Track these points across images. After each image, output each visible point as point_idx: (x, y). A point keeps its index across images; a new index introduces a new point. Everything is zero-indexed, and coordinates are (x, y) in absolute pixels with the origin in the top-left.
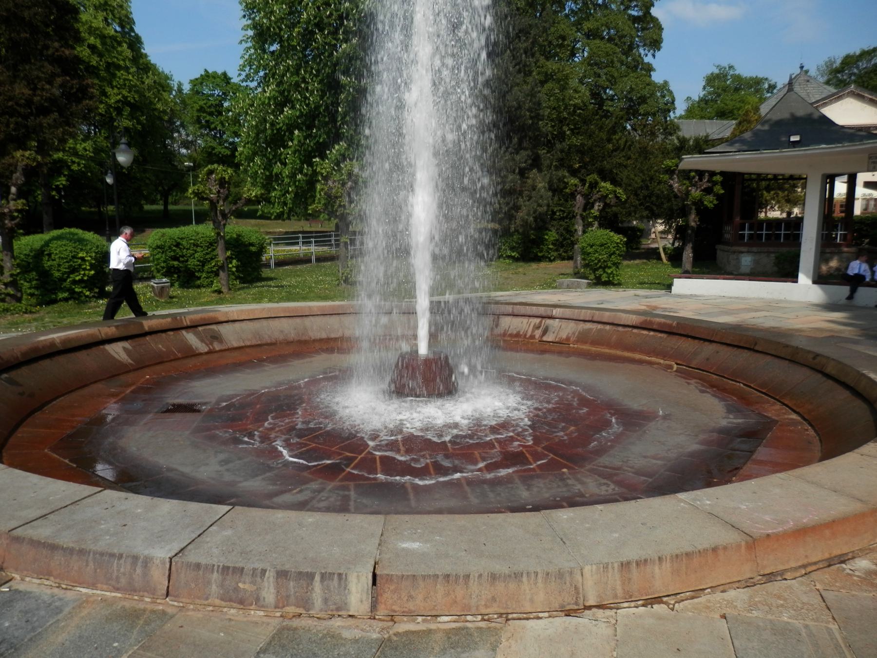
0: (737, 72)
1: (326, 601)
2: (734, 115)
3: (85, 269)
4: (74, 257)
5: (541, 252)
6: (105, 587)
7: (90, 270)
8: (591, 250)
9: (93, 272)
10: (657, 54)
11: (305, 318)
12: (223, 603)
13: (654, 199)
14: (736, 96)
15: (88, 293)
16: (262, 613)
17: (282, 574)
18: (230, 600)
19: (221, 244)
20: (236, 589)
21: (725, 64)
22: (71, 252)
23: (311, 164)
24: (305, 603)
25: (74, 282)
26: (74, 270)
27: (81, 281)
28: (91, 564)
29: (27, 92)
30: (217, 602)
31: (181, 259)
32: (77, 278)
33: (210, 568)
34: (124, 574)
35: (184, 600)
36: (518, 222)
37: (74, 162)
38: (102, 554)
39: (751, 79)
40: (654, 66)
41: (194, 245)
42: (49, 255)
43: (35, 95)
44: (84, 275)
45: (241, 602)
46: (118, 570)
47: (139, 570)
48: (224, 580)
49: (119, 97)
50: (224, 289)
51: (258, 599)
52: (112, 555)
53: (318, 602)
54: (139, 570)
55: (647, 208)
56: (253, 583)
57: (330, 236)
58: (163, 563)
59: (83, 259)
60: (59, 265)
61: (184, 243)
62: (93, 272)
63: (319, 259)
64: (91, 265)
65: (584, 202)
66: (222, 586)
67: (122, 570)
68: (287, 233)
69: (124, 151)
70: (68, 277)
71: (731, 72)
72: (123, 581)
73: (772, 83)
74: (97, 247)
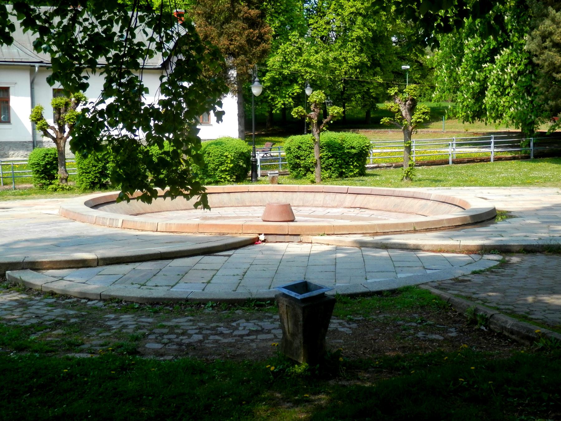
3: (227, 163)
4: (221, 155)
7: (230, 164)
9: (232, 165)
15: (229, 178)
17: (110, 219)
19: (316, 148)
22: (220, 152)
23: (481, 69)
25: (222, 171)
26: (222, 164)
27: (225, 171)
29: (227, 42)
31: (301, 158)
32: (223, 169)
37: (307, 72)
41: (310, 148)
42: (209, 154)
43: (231, 44)
44: (227, 166)
49: (353, 9)
50: (317, 180)
57: (490, 138)
59: (226, 156)
60: (214, 160)
61: (303, 146)
62: (232, 165)
63: (458, 161)
64: (231, 160)
68: (484, 134)
69: (256, 86)
70: (218, 168)
74: (236, 149)
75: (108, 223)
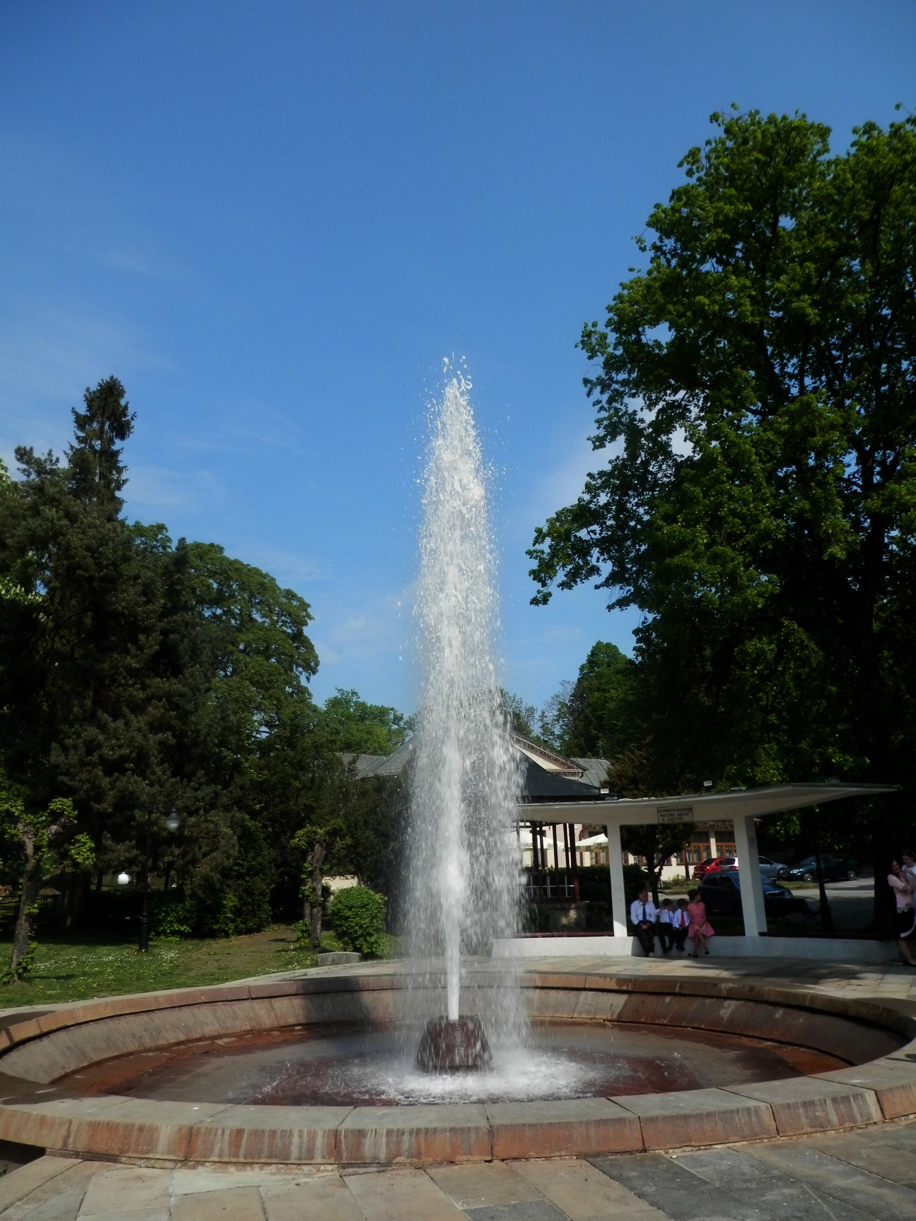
0: (361, 700)
1: (861, 1114)
2: (361, 747)
5: (217, 922)
6: (735, 1138)
8: (349, 914)
10: (312, 678)
11: (152, 1015)
12: (813, 1130)
13: (360, 849)
14: (361, 726)
16: (833, 1132)
18: (815, 1126)
20: (816, 1117)
21: (347, 688)
24: (852, 1119)
28: (719, 1122)
30: (809, 1130)
33: (796, 1105)
34: (745, 1124)
35: (789, 1134)
36: (197, 881)
38: (724, 1113)
39: (377, 708)
40: (311, 690)
45: (822, 1126)
46: (740, 1123)
47: (754, 1119)
48: (807, 1112)
51: (829, 1122)
52: (732, 1112)
53: (858, 1116)
54: (754, 1119)
55: (351, 862)
56: (823, 1110)
58: (767, 1109)
65: (324, 852)
66: (807, 1117)
67: (743, 1121)
71: (355, 699)
72: (747, 1131)
73: (399, 714)
75: (834, 1118)
